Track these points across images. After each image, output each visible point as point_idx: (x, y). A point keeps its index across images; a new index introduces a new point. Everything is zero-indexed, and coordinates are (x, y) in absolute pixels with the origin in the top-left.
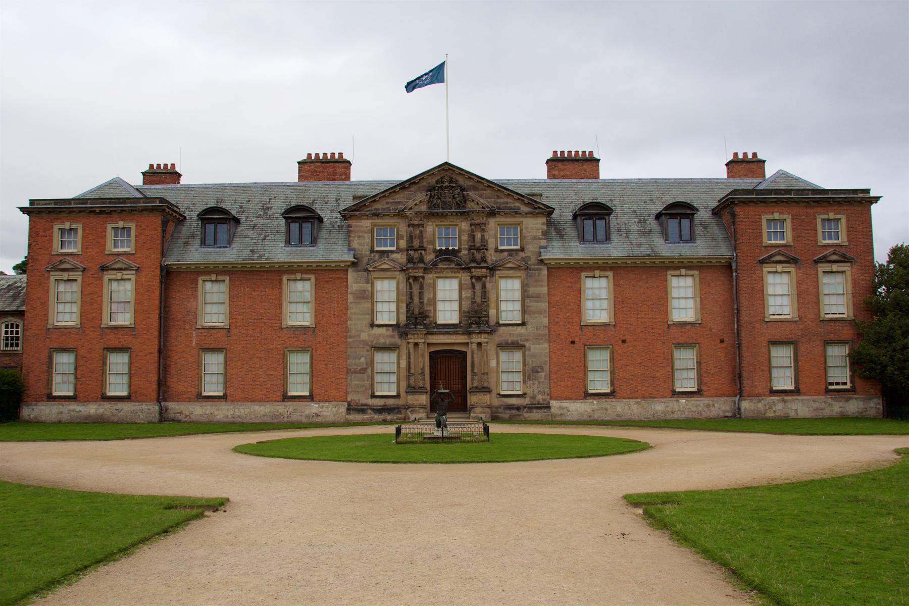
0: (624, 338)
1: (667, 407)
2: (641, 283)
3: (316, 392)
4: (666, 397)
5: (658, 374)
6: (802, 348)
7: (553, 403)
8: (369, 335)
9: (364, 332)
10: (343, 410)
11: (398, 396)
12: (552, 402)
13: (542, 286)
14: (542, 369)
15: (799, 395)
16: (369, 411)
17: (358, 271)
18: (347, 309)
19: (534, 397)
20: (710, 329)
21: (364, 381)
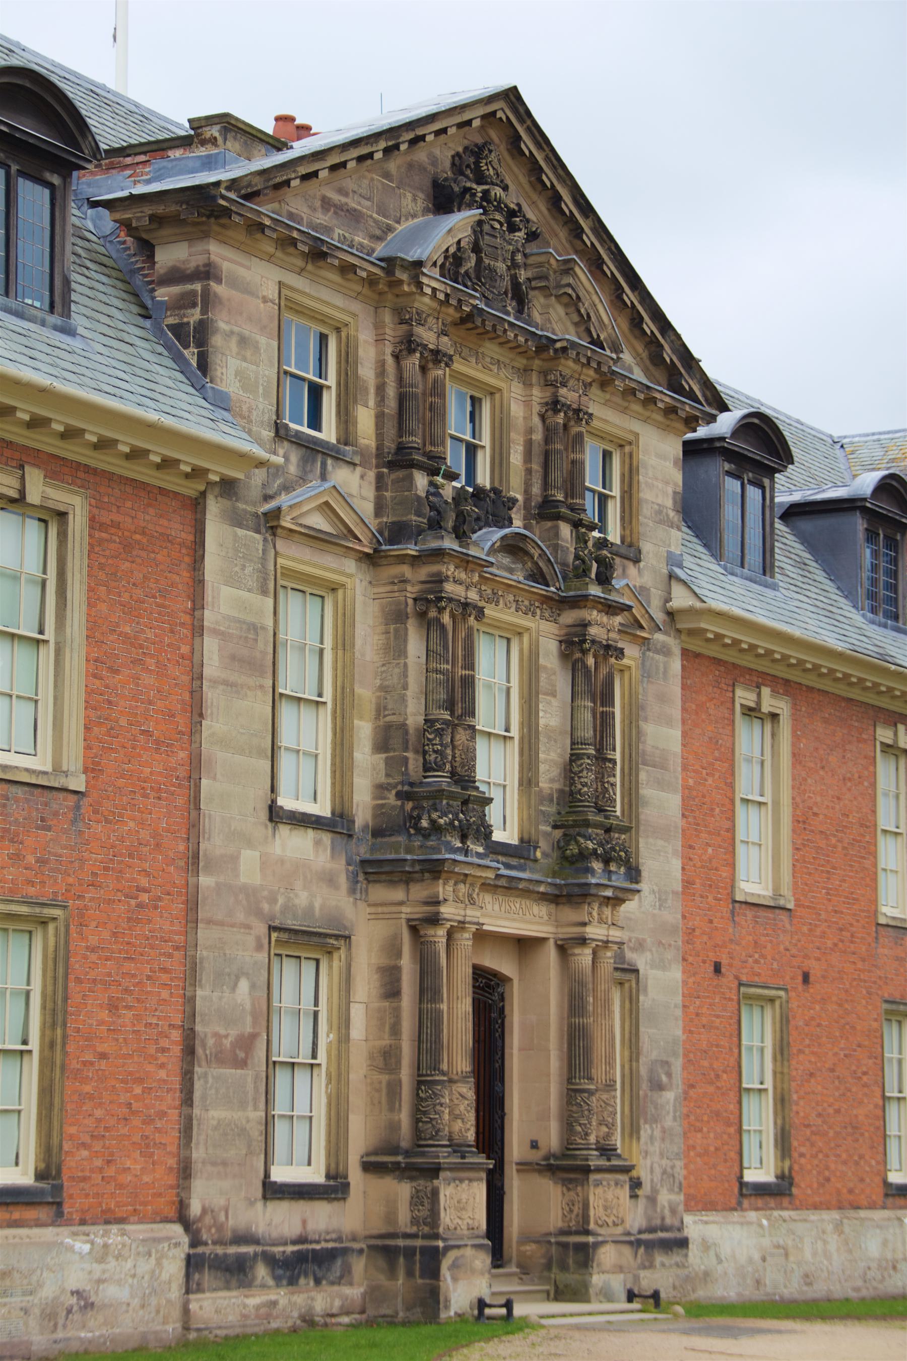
1: (885, 1243)
3: (75, 1161)
7: (694, 1226)
8: (264, 863)
9: (249, 843)
10: (173, 1268)
11: (334, 1189)
12: (688, 1219)
13: (669, 723)
16: (261, 1272)
17: (240, 525)
18: (197, 710)
19: (652, 1200)
21: (243, 1105)
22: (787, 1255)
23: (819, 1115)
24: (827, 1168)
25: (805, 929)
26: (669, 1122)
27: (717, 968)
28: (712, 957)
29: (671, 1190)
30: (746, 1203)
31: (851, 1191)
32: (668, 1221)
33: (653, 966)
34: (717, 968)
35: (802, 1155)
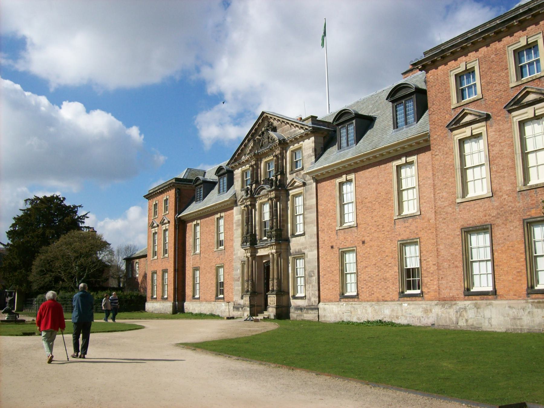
0: (363, 239)
1: (393, 310)
2: (373, 181)
4: (394, 300)
5: (388, 275)
6: (497, 232)
7: (321, 305)
14: (314, 274)
15: (496, 299)
20: (429, 220)
22: (351, 313)
23: (370, 277)
24: (373, 291)
25: (363, 230)
26: (314, 283)
27: (332, 247)
28: (331, 245)
29: (315, 298)
30: (342, 300)
31: (383, 297)
32: (314, 304)
33: (309, 251)
34: (332, 247)
35: (362, 288)
